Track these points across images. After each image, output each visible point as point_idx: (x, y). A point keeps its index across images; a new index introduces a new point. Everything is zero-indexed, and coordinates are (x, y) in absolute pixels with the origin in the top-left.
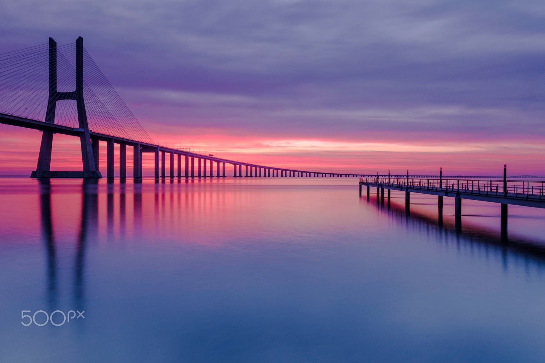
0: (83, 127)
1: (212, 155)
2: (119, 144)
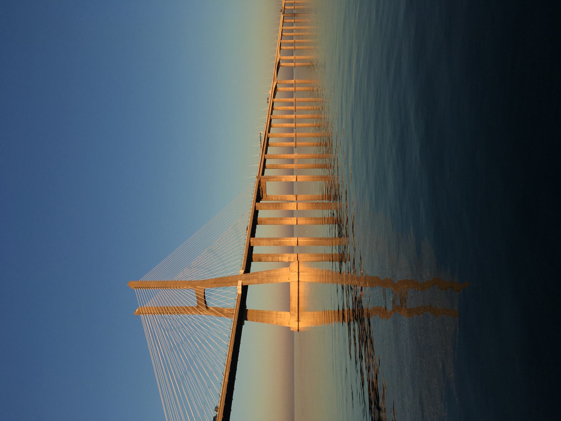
0: (237, 282)
1: (268, 99)
2: (257, 225)
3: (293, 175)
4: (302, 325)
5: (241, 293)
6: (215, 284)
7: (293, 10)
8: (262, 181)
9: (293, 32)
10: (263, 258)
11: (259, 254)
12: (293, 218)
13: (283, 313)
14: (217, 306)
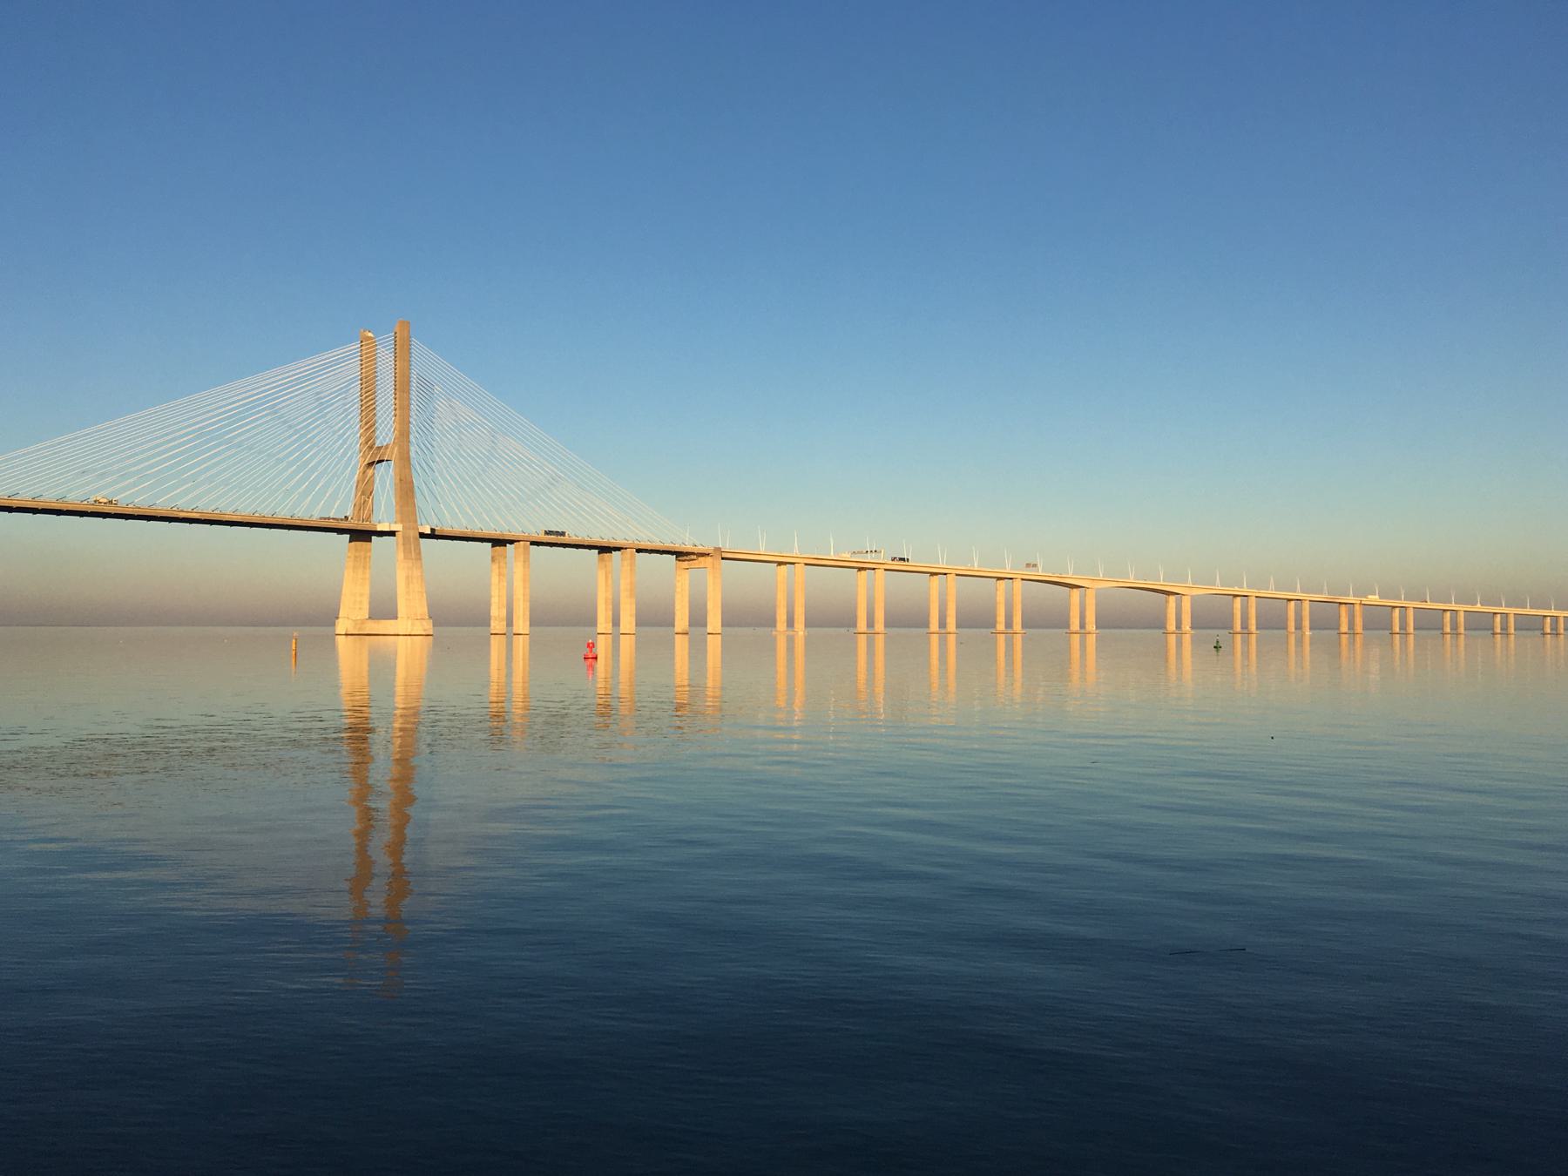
0: (402, 521)
3: (722, 626)
4: (341, 640)
5: (379, 530)
6: (398, 481)
7: (1438, 629)
8: (709, 559)
9: (1296, 629)
10: (495, 566)
11: (506, 557)
12: (611, 624)
13: (366, 606)
14: (378, 479)
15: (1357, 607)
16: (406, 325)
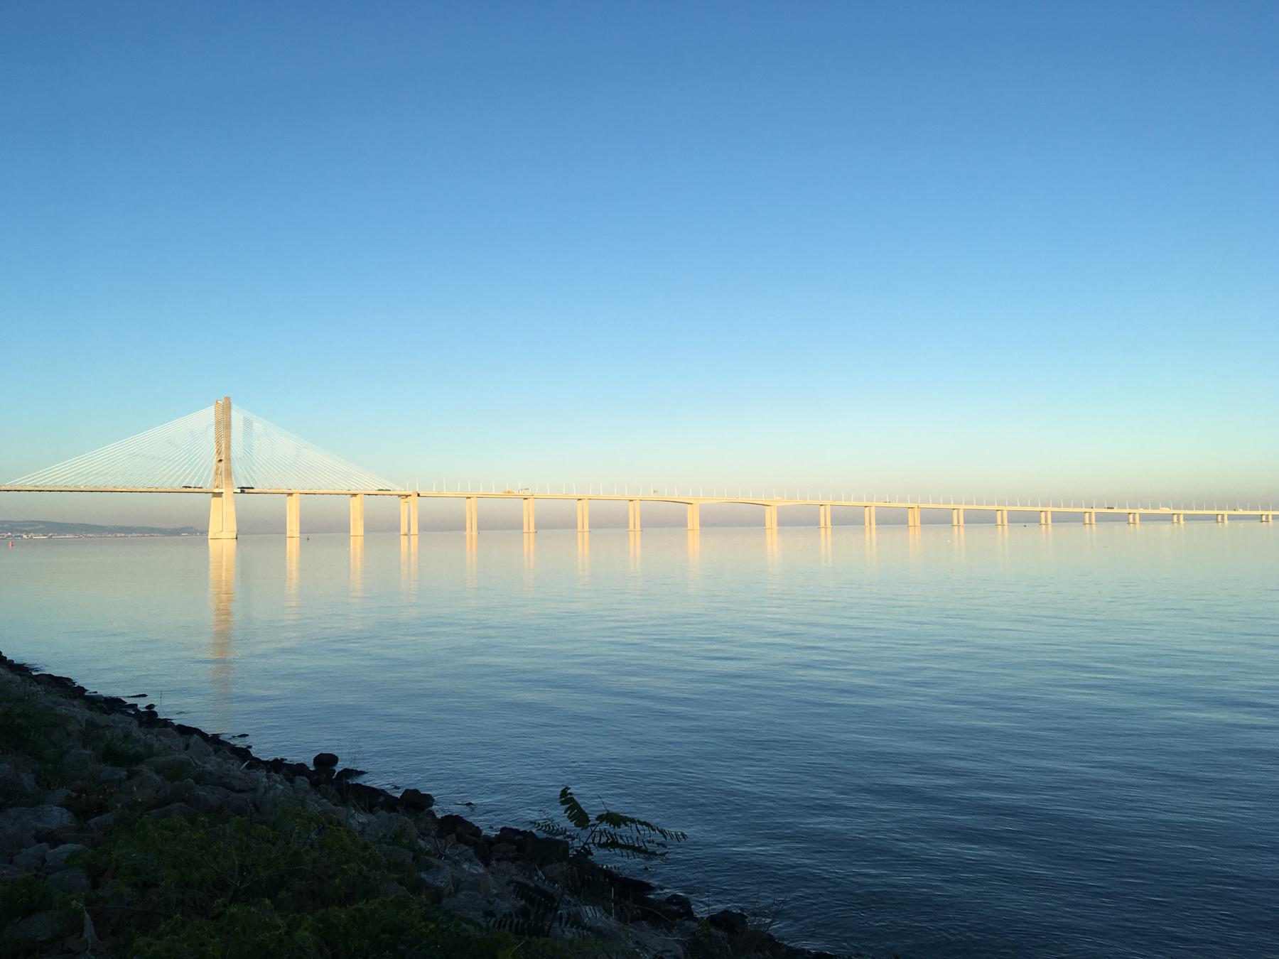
4: (210, 541)
15: (916, 509)
16: (227, 399)
